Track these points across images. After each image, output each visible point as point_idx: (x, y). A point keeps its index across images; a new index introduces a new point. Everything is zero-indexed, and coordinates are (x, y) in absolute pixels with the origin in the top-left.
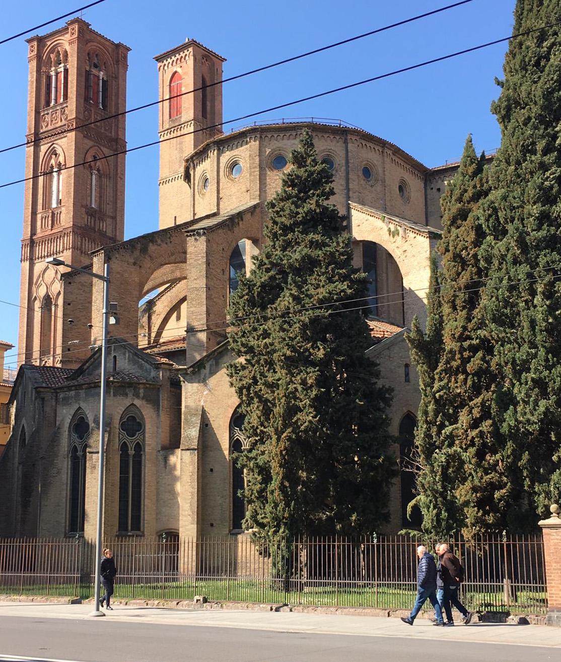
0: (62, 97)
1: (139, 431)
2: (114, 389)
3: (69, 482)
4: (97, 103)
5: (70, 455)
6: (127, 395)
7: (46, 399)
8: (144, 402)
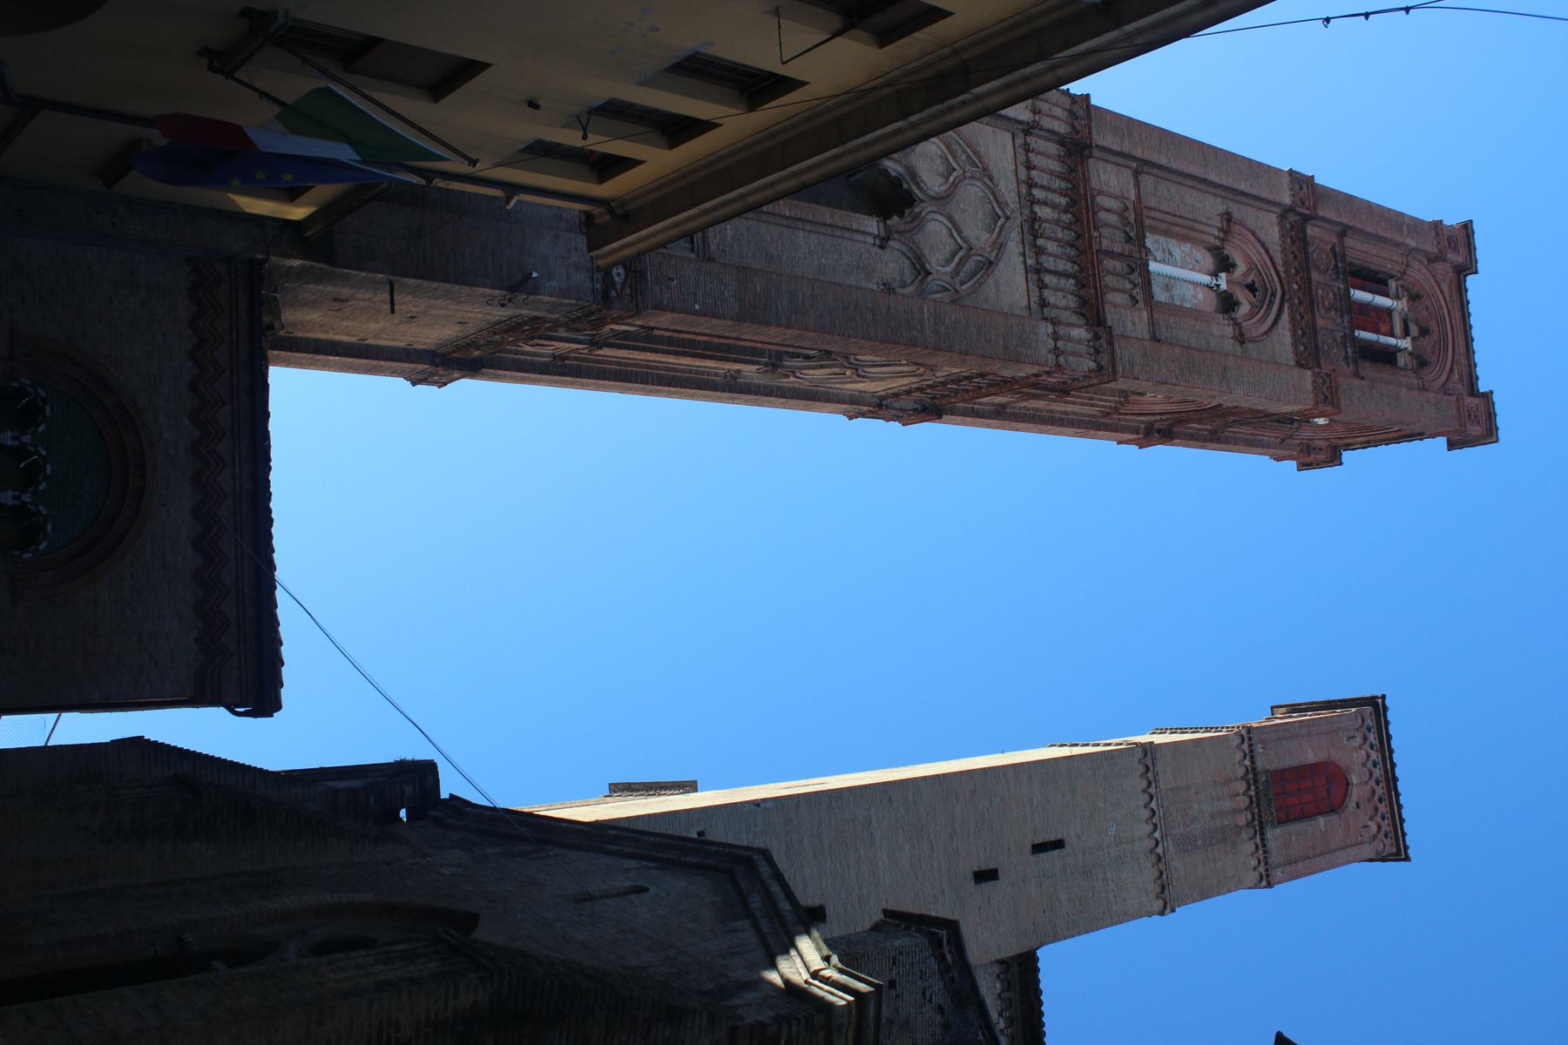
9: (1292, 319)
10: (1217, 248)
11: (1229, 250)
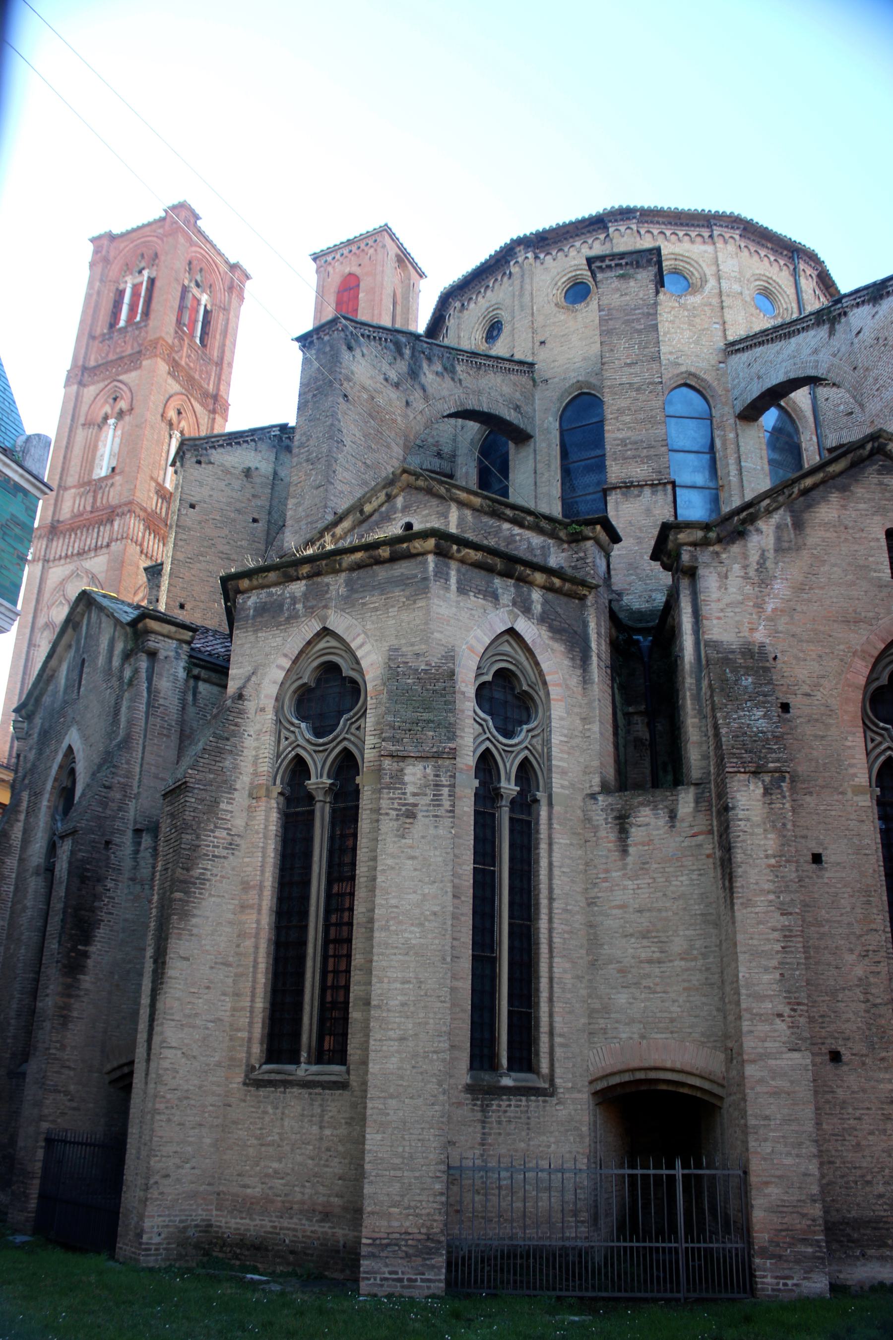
1: (527, 723)
2: (458, 571)
4: (192, 336)
5: (278, 788)
6: (494, 597)
7: (162, 655)
8: (545, 633)
11: (100, 419)
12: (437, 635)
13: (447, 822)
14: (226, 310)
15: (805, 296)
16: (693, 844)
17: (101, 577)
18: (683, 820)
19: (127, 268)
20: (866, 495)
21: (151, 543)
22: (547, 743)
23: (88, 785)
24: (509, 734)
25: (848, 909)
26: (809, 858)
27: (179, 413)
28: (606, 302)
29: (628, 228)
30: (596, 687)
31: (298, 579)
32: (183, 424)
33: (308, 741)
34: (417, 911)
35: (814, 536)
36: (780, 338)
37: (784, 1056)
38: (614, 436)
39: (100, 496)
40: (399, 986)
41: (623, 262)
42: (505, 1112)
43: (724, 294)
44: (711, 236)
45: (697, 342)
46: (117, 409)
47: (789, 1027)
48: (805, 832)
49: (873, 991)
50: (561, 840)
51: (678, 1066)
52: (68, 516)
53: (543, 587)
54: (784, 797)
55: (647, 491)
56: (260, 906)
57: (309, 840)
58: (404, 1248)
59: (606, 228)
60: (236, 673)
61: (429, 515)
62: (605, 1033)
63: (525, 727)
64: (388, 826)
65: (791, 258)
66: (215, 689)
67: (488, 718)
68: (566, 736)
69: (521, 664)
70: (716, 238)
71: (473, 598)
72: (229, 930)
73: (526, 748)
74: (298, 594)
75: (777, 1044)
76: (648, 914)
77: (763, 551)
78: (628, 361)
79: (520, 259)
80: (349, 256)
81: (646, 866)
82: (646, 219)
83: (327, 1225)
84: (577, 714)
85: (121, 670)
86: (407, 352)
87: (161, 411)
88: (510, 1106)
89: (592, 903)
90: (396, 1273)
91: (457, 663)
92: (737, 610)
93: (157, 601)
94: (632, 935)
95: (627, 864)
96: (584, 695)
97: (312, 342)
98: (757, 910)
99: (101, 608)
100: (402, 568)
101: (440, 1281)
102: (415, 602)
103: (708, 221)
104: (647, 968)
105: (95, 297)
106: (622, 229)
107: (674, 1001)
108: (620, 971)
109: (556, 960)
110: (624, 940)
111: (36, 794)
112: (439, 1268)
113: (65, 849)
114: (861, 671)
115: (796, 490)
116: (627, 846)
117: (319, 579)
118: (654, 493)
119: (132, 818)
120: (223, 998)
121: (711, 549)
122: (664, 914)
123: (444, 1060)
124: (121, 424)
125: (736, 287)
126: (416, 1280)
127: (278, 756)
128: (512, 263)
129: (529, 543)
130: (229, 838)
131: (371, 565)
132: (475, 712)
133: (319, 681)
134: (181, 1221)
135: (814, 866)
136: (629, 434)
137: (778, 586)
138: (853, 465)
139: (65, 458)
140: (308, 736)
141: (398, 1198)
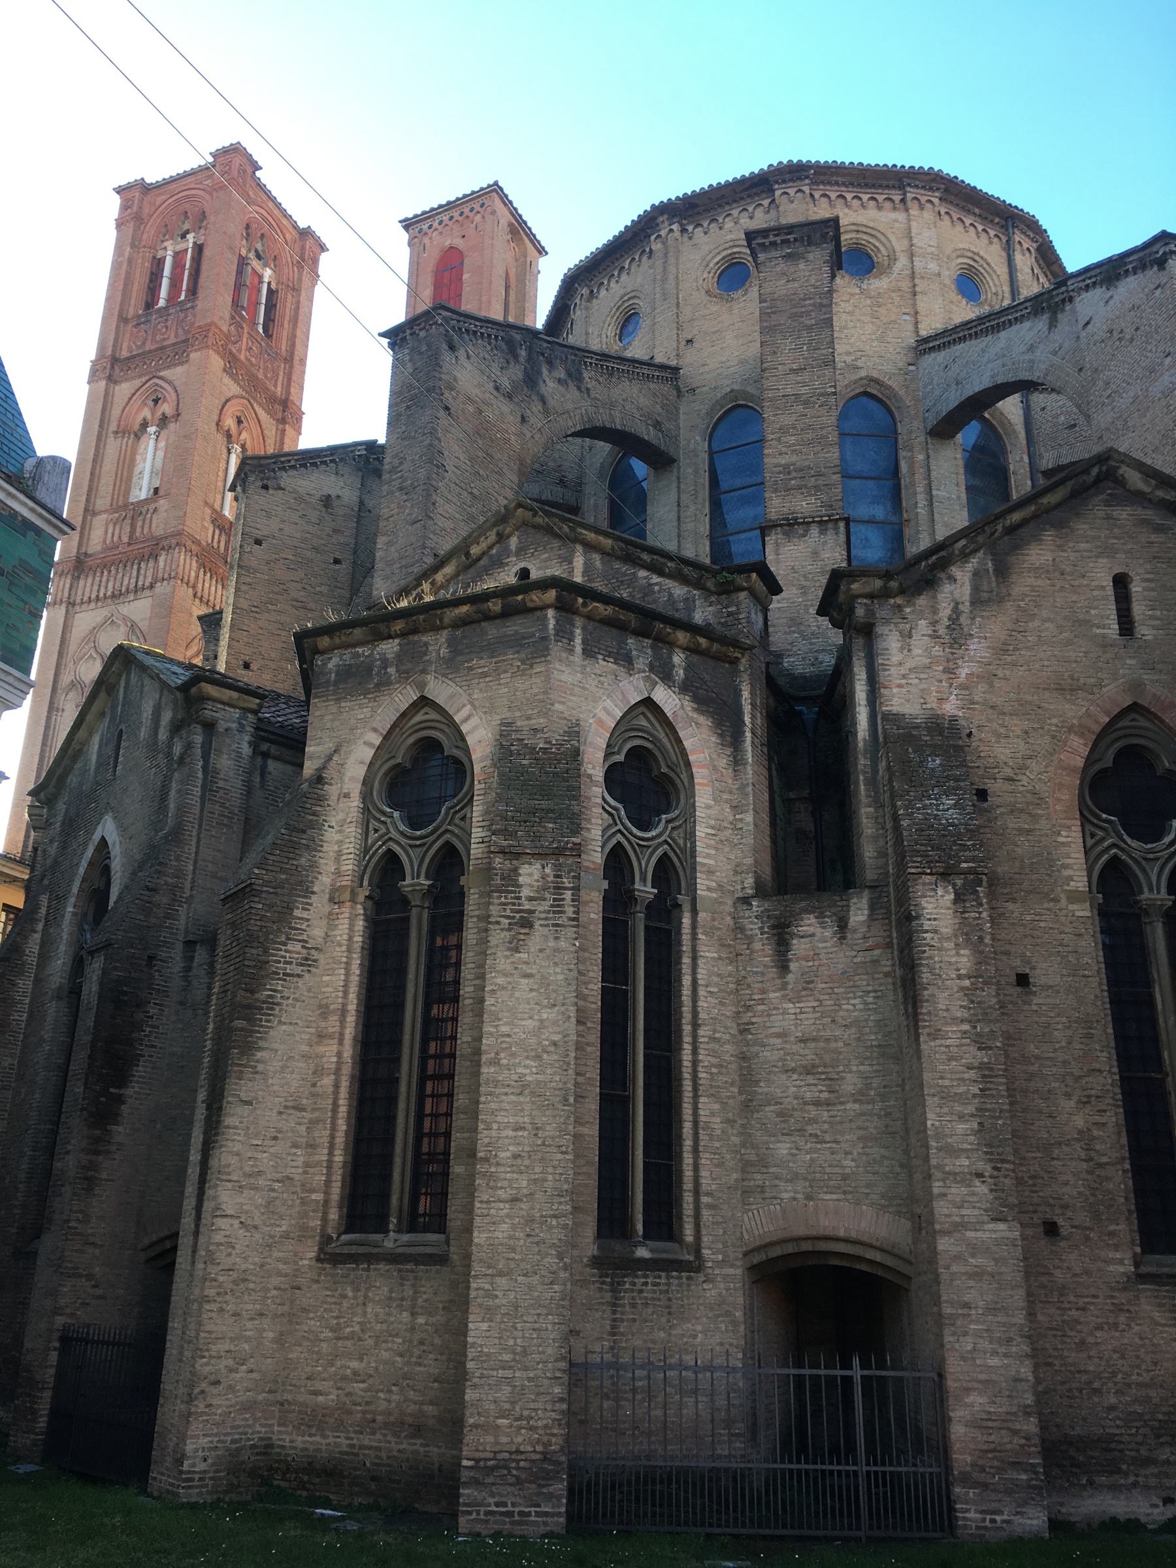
0: (183, 293)
2: (584, 629)
3: (352, 1007)
4: (255, 324)
6: (626, 661)
7: (221, 726)
8: (689, 705)
9: (168, 367)
10: (136, 435)
11: (136, 427)
12: (558, 706)
13: (570, 932)
14: (296, 290)
15: (1020, 277)
16: (868, 959)
17: (143, 626)
18: (855, 931)
19: (167, 231)
20: (1089, 533)
21: (207, 585)
22: (691, 836)
23: (126, 887)
24: (645, 827)
25: (1063, 1044)
26: (1013, 979)
27: (239, 422)
28: (769, 290)
29: (800, 191)
30: (749, 768)
31: (390, 637)
32: (244, 435)
33: (402, 833)
34: (533, 1041)
35: (1023, 584)
36: (986, 332)
37: (986, 1227)
38: (775, 461)
39: (139, 524)
40: (511, 1133)
41: (791, 237)
42: (641, 1291)
43: (917, 275)
44: (903, 201)
45: (881, 339)
46: (159, 414)
47: (991, 1190)
48: (1008, 947)
49: (1098, 1147)
50: (708, 952)
51: (853, 1235)
52: (99, 548)
53: (686, 649)
54: (981, 905)
55: (814, 531)
56: (342, 1035)
57: (403, 954)
58: (514, 1472)
59: (772, 191)
60: (315, 750)
61: (549, 559)
62: (763, 1192)
63: (664, 816)
64: (498, 937)
65: (1005, 228)
66: (289, 769)
67: (620, 806)
68: (712, 828)
69: (660, 741)
70: (909, 203)
71: (601, 662)
72: (303, 1065)
73: (666, 842)
74: (390, 656)
75: (976, 1212)
76: (813, 1045)
77: (957, 603)
78: (795, 366)
79: (663, 233)
80: (450, 223)
81: (811, 986)
82: (822, 178)
83: (419, 1442)
84: (727, 801)
85: (170, 745)
86: (523, 353)
87: (216, 418)
88: (646, 1284)
89: (746, 1030)
90: (505, 1505)
91: (582, 740)
92: (922, 676)
93: (216, 657)
94: (793, 1070)
95: (787, 983)
96: (735, 777)
97: (404, 339)
98: (948, 1042)
99: (143, 668)
100: (516, 626)
101: (559, 1514)
102: (531, 666)
103: (900, 180)
104: (813, 1112)
105: (125, 267)
106: (791, 191)
107: (846, 1153)
108: (780, 1114)
109: (702, 1100)
110: (784, 1077)
111: (58, 898)
112: (559, 1498)
113: (95, 968)
114: (1077, 751)
115: (1000, 528)
116: (789, 960)
117: (416, 638)
118: (823, 532)
119: (182, 927)
120: (294, 1150)
121: (892, 601)
122: (833, 1045)
123: (565, 1226)
124: (164, 433)
125: (933, 267)
126: (529, 1514)
127: (366, 851)
128: (653, 238)
129: (670, 594)
130: (305, 951)
131: (479, 621)
132: (604, 799)
133: (415, 761)
134: (233, 1441)
135: (1019, 989)
136: (794, 458)
137: (975, 646)
138: (1074, 495)
139: (92, 474)
140: (402, 827)
141: (507, 1406)
